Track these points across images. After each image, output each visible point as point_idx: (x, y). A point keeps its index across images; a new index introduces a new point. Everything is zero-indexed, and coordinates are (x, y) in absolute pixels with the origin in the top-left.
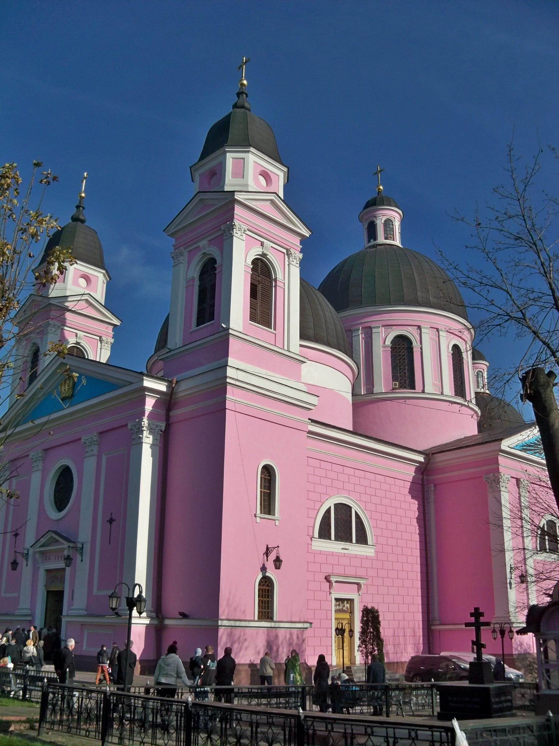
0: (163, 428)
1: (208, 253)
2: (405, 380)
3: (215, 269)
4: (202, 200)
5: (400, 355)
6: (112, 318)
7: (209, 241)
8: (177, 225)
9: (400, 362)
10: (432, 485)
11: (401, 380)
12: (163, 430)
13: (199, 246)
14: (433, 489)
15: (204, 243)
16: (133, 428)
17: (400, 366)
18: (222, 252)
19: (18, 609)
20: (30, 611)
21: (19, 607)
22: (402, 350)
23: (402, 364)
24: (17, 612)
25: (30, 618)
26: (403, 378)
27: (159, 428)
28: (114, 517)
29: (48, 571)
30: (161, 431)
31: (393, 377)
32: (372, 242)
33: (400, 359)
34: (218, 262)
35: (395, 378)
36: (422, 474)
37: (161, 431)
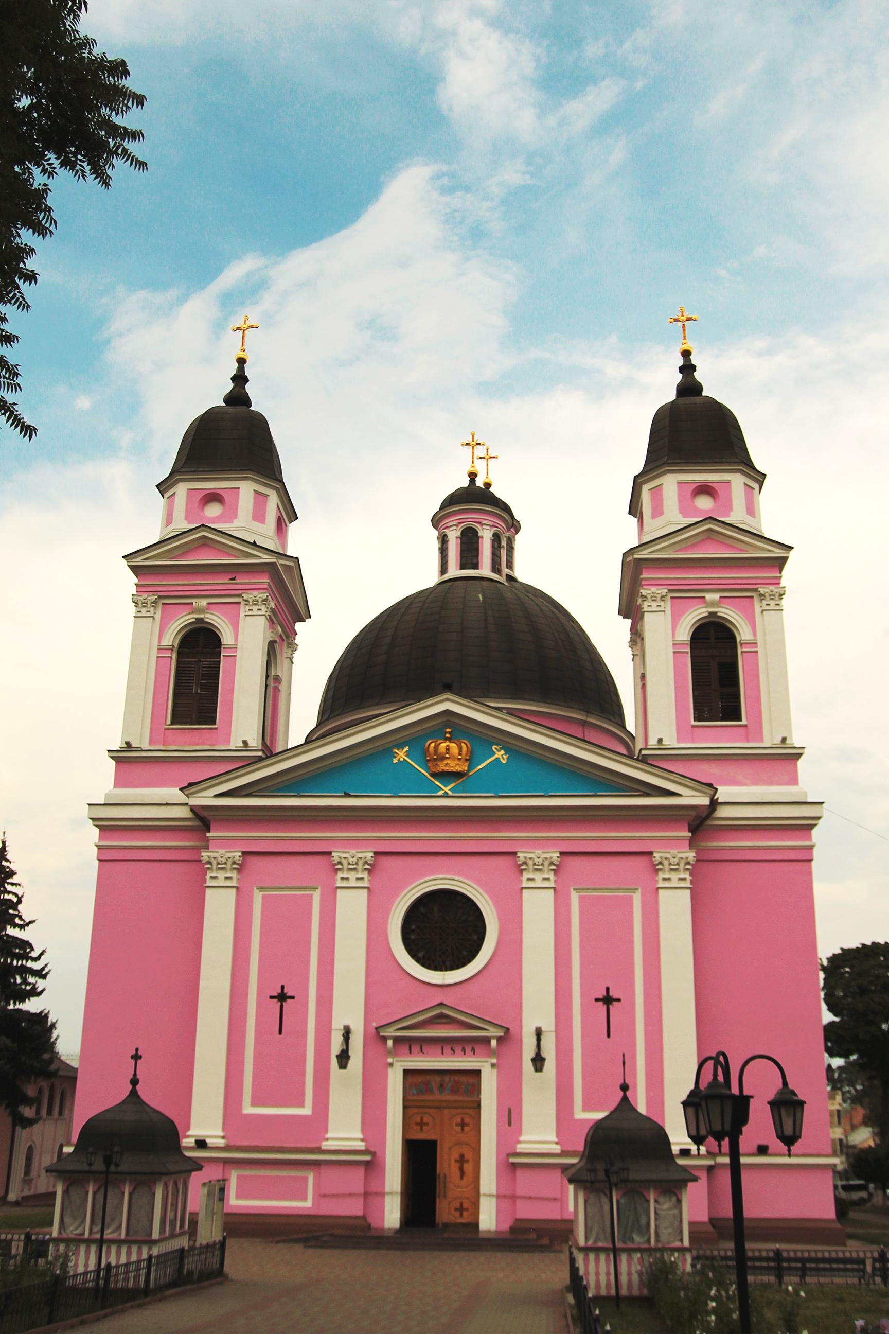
1: (719, 614)
4: (710, 530)
7: (721, 597)
13: (704, 597)
19: (327, 1139)
20: (363, 1144)
21: (328, 1136)
24: (326, 1145)
25: (368, 1158)
28: (614, 994)
29: (407, 1072)
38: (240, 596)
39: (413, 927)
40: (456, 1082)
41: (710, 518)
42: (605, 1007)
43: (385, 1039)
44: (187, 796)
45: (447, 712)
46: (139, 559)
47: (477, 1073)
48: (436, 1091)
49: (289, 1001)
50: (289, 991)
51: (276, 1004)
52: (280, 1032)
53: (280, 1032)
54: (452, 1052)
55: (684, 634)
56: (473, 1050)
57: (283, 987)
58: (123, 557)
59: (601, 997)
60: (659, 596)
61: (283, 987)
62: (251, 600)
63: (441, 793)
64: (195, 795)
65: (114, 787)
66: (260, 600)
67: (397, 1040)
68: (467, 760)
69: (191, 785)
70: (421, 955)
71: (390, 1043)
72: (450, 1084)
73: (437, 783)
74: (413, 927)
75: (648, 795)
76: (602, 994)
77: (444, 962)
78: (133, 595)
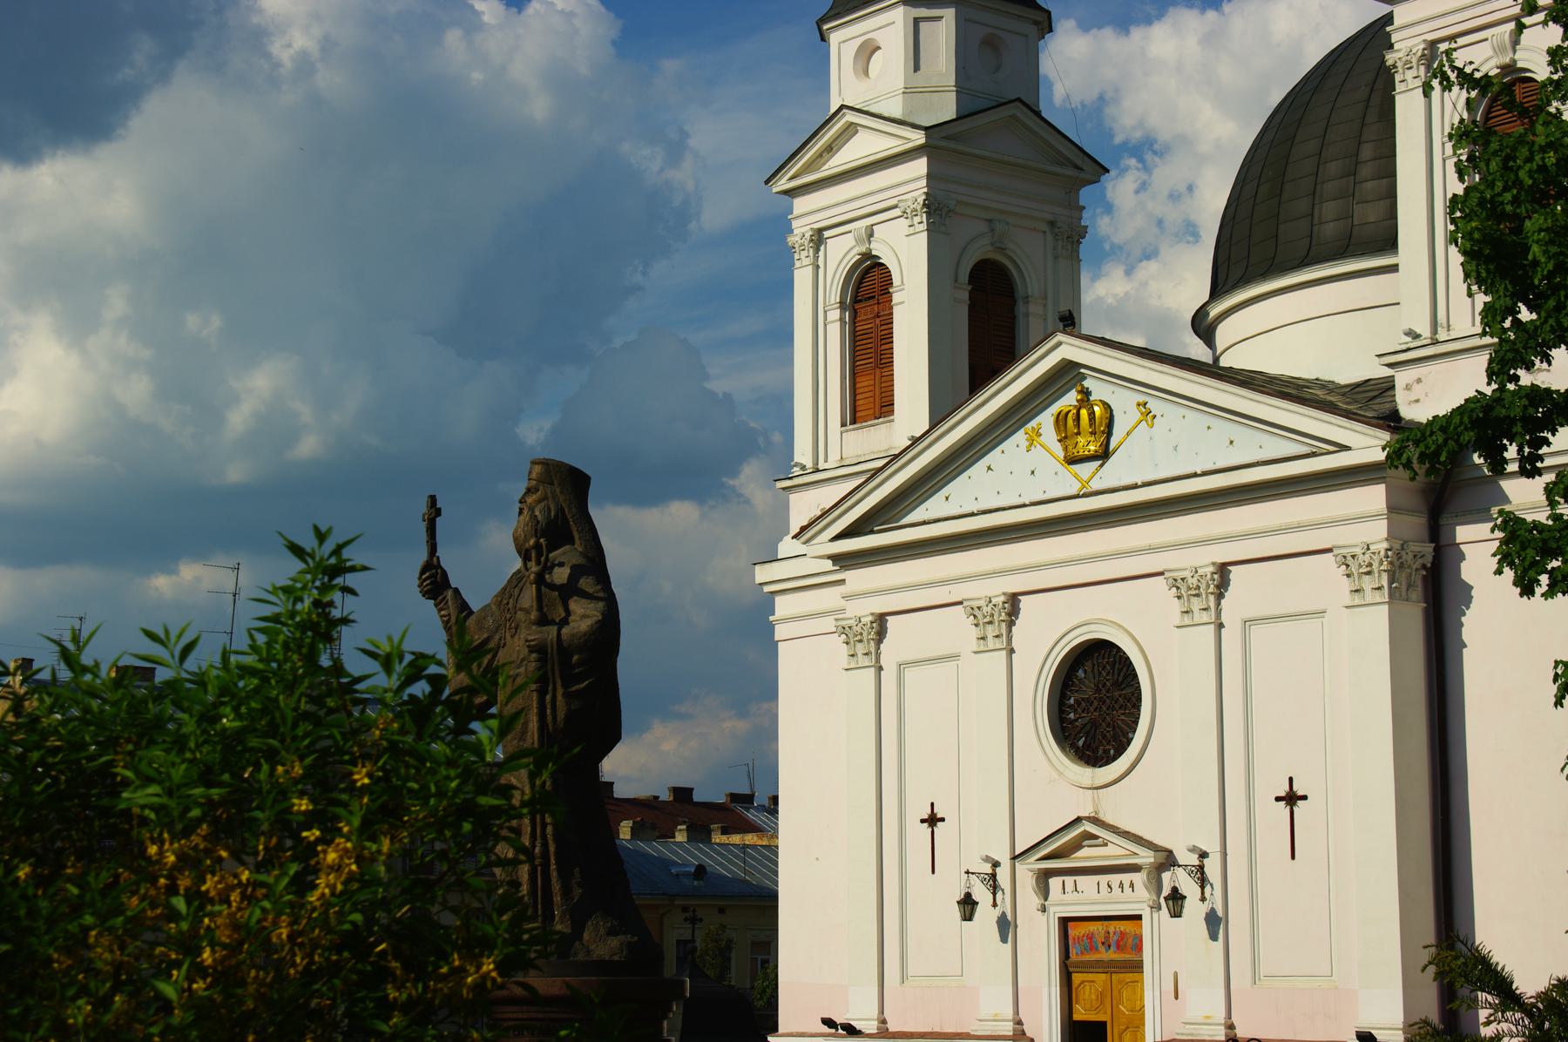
0: (1428, 560)
6: (1079, 163)
12: (1429, 565)
16: (1350, 561)
27: (1420, 561)
30: (1424, 567)
38: (895, 207)
39: (1072, 701)
40: (1123, 934)
42: (1288, 807)
44: (804, 543)
46: (784, 181)
47: (1139, 917)
48: (1102, 949)
54: (1109, 890)
56: (1132, 885)
59: (1283, 794)
60: (1414, 60)
62: (909, 211)
64: (813, 542)
66: (919, 208)
68: (1103, 432)
69: (803, 529)
70: (1081, 743)
72: (1115, 938)
74: (1072, 701)
75: (1314, 455)
76: (1283, 790)
77: (1106, 752)
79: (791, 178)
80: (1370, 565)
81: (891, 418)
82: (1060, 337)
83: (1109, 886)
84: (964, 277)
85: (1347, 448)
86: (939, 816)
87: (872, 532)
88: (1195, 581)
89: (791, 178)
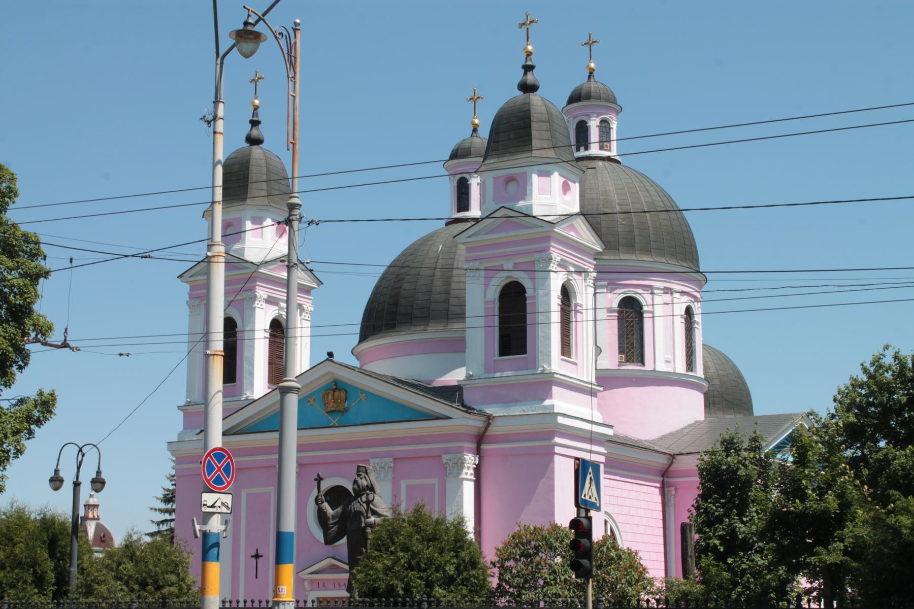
0: (477, 462)
2: (633, 353)
3: (525, 299)
5: (627, 321)
7: (515, 264)
8: (473, 235)
9: (627, 330)
10: (673, 488)
11: (628, 352)
14: (673, 493)
15: (508, 265)
16: (449, 462)
17: (627, 335)
18: (534, 284)
22: (629, 315)
23: (630, 332)
26: (630, 350)
31: (620, 348)
32: (583, 153)
33: (627, 326)
34: (529, 293)
35: (621, 351)
36: (663, 476)
37: (475, 464)
41: (503, 207)
43: (304, 580)
45: (329, 372)
49: (260, 558)
50: (260, 553)
51: (254, 560)
52: (256, 577)
53: (256, 577)
55: (494, 293)
57: (257, 550)
58: (178, 277)
61: (257, 550)
62: (248, 298)
63: (331, 424)
65: (185, 427)
67: (312, 581)
71: (306, 584)
73: (330, 418)
78: (187, 301)
79: (191, 277)
80: (456, 463)
81: (234, 384)
82: (327, 362)
83: (339, 585)
84: (268, 328)
85: (450, 418)
86: (260, 554)
87: (234, 434)
88: (383, 464)
89: (191, 277)
